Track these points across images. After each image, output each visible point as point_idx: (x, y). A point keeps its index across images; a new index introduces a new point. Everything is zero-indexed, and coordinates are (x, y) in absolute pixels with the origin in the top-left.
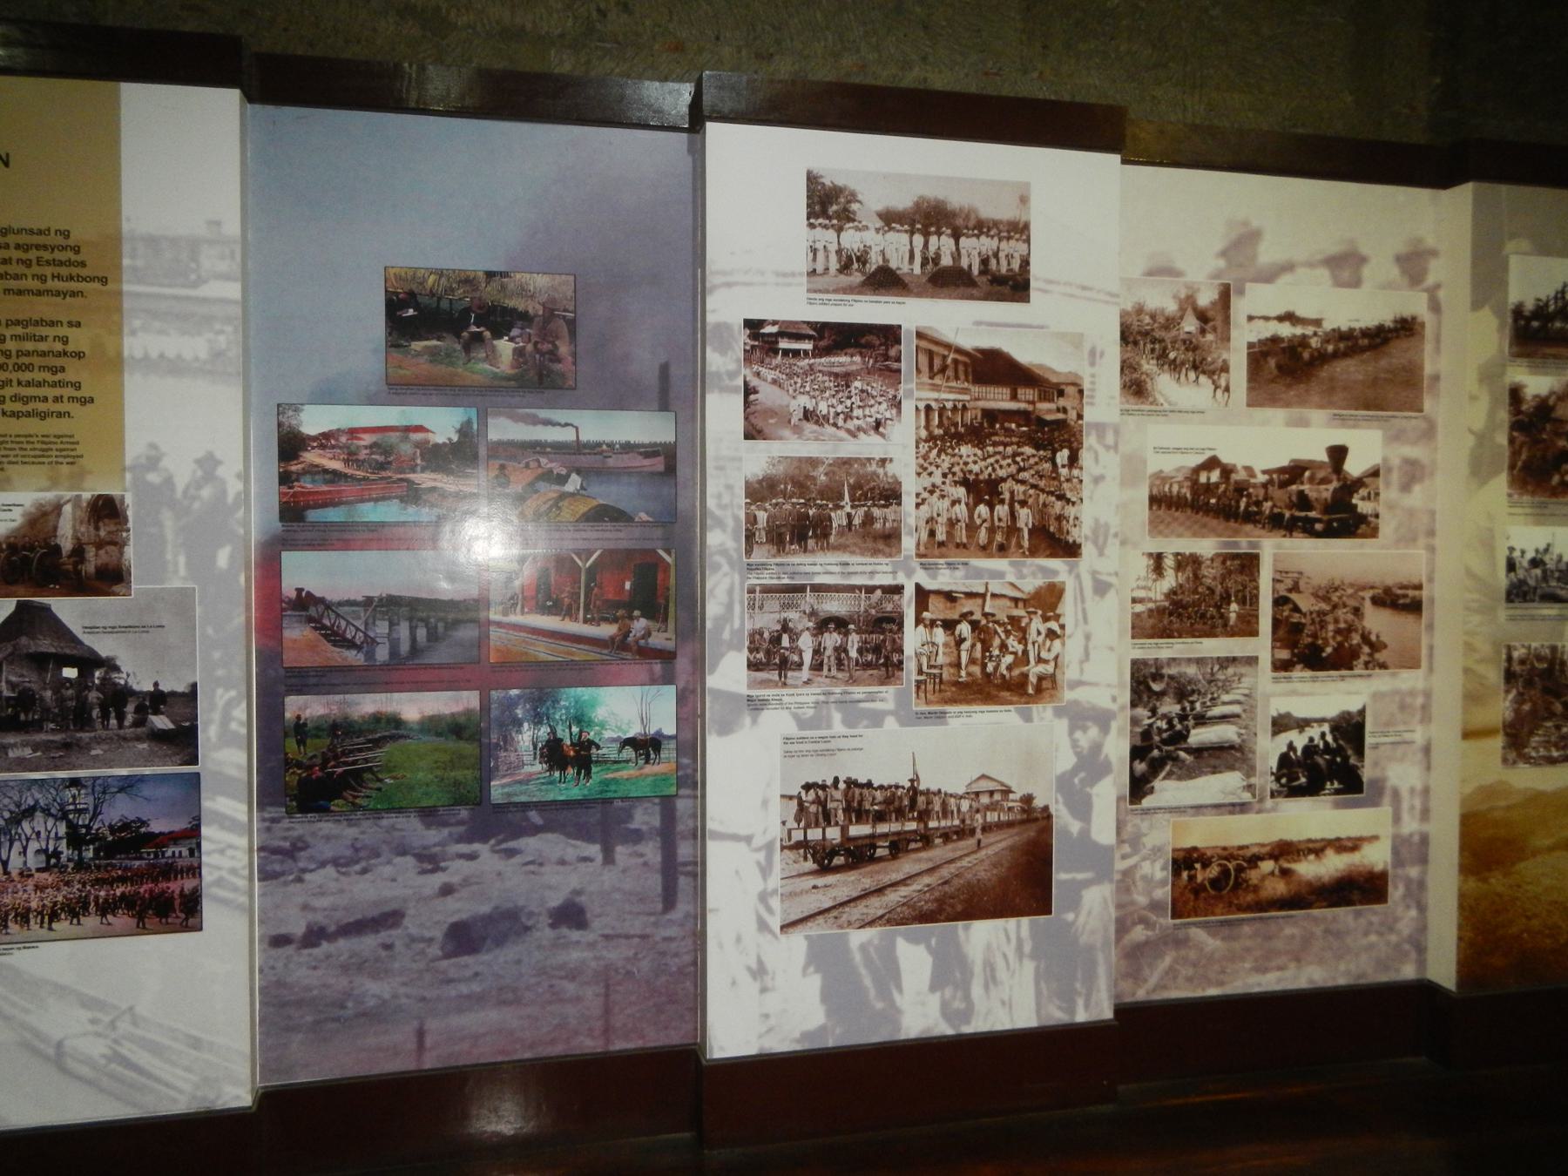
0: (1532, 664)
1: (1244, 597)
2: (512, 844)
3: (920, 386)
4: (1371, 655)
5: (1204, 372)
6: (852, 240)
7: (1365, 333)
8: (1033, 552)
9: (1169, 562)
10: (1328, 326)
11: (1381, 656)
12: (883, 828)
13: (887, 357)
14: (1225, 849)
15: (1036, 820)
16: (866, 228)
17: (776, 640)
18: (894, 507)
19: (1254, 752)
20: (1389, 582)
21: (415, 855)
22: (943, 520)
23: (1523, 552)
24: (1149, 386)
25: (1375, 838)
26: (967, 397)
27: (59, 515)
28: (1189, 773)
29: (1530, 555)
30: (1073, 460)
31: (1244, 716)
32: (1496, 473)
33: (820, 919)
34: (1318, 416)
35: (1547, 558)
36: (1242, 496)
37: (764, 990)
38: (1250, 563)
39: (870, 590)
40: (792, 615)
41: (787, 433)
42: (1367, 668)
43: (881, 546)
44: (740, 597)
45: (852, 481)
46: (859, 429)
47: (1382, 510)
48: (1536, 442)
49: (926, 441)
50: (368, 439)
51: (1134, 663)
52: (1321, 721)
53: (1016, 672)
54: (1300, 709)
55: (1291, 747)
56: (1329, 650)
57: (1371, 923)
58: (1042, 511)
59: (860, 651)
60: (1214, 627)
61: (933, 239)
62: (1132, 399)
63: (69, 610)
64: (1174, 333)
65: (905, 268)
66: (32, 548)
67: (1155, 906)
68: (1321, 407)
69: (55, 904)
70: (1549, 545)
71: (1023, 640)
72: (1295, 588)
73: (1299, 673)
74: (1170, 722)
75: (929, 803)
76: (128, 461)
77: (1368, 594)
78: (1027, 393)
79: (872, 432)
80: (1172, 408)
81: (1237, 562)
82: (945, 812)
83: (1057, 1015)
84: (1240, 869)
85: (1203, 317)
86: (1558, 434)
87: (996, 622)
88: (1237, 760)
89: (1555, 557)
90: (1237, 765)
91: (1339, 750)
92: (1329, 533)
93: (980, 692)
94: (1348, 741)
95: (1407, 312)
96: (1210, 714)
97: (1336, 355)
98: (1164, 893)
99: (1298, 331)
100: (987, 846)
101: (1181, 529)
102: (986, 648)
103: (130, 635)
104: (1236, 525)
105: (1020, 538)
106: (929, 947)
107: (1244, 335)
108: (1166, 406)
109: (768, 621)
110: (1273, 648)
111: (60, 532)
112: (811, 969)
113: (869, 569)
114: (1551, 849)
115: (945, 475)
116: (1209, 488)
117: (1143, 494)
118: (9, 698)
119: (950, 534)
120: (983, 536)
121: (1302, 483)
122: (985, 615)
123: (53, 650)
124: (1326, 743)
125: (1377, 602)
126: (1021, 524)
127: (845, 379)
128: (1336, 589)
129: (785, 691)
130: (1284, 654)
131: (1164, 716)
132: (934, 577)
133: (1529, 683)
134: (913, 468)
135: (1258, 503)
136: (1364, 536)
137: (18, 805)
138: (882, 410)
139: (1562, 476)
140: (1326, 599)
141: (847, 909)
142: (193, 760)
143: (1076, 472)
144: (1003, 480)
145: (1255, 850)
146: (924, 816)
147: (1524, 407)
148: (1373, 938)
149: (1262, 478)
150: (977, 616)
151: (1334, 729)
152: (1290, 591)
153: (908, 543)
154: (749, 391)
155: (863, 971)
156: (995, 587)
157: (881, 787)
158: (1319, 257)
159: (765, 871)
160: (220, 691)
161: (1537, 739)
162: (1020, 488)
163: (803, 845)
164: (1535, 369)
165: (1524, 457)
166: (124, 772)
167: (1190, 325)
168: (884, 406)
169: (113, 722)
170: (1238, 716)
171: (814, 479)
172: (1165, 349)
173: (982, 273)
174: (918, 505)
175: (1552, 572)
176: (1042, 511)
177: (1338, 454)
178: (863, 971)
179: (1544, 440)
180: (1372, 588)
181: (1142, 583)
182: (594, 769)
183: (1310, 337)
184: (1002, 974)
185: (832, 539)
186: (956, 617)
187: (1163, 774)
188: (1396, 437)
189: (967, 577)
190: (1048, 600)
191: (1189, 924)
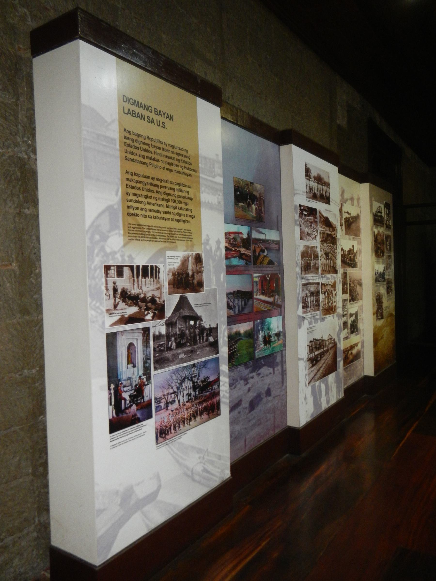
17: (306, 299)
22: (323, 264)
26: (325, 230)
27: (188, 261)
30: (336, 247)
37: (306, 404)
39: (316, 283)
44: (301, 286)
63: (191, 297)
66: (182, 274)
69: (190, 414)
76: (203, 241)
103: (204, 307)
111: (189, 268)
118: (179, 334)
119: (324, 267)
123: (188, 314)
127: (311, 223)
132: (323, 280)
137: (181, 378)
142: (217, 353)
150: (328, 291)
157: (319, 340)
160: (222, 326)
162: (331, 255)
166: (203, 359)
169: (201, 340)
171: (308, 252)
176: (333, 262)
182: (271, 344)
189: (326, 280)
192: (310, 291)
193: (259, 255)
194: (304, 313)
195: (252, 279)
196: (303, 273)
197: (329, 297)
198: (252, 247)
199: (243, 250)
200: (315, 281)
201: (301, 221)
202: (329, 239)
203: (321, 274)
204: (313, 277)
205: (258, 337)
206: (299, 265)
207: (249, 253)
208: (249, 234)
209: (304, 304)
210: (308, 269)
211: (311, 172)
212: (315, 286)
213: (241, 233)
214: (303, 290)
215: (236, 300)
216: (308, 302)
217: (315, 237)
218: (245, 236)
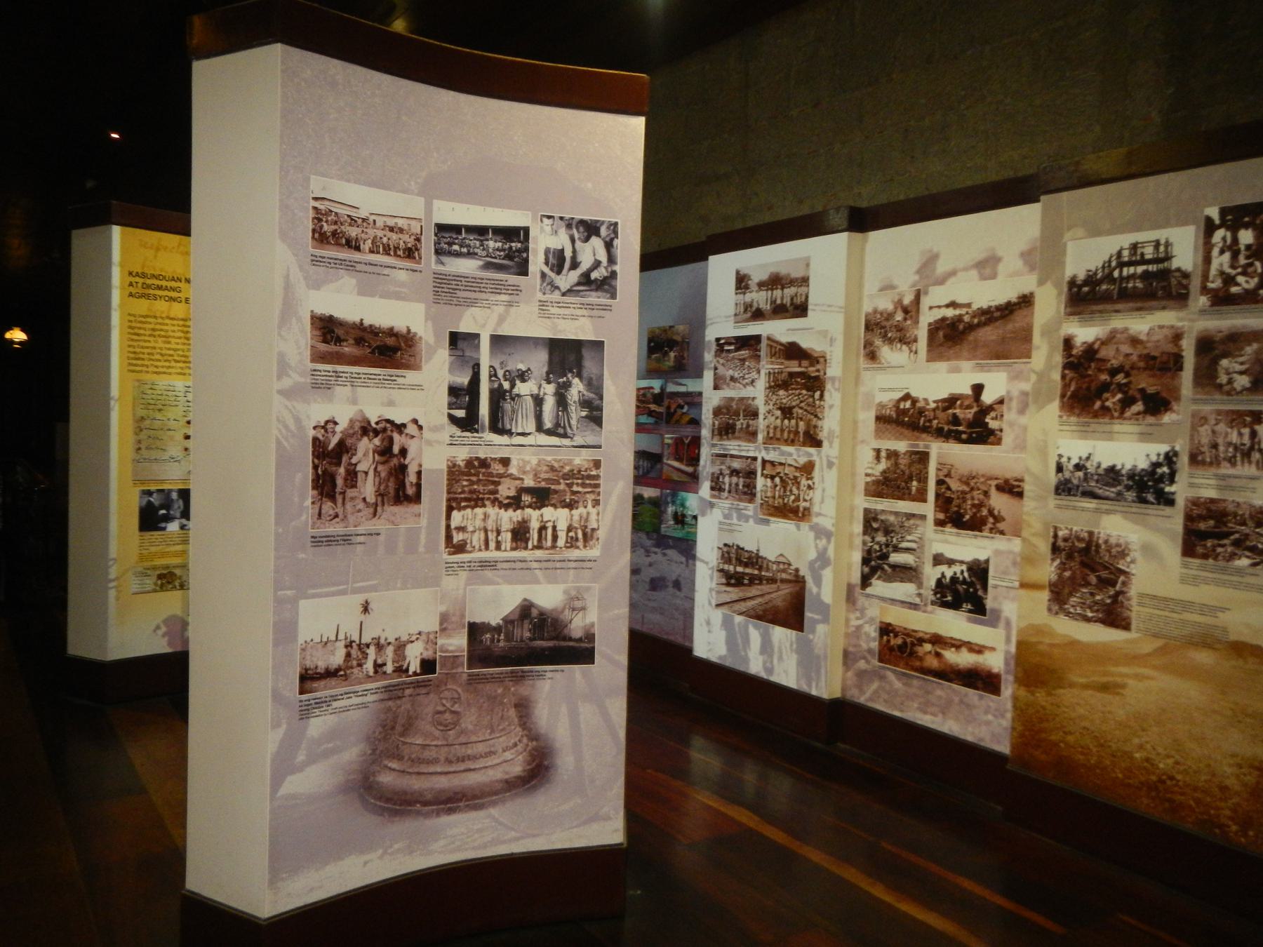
0: (1073, 543)
1: (920, 478)
4: (994, 524)
5: (905, 343)
6: (748, 297)
7: (998, 308)
8: (804, 444)
9: (883, 454)
10: (975, 307)
11: (1001, 526)
12: (748, 571)
14: (905, 629)
15: (799, 581)
17: (718, 478)
19: (922, 573)
20: (1008, 476)
22: (772, 426)
23: (1069, 459)
24: (878, 354)
25: (993, 649)
28: (889, 579)
29: (1075, 461)
30: (822, 396)
31: (918, 550)
32: (1050, 401)
33: (726, 606)
34: (966, 365)
35: (1088, 465)
36: (921, 416)
37: (709, 631)
38: (923, 457)
39: (747, 458)
40: (723, 467)
41: (725, 386)
42: (991, 533)
43: (751, 438)
45: (743, 407)
46: (747, 384)
47: (1005, 427)
48: (1083, 376)
51: (867, 511)
52: (962, 562)
53: (795, 505)
54: (950, 553)
55: (943, 575)
56: (967, 517)
57: (989, 707)
58: (808, 423)
59: (744, 486)
60: (904, 494)
62: (870, 362)
64: (891, 322)
67: (870, 651)
68: (969, 359)
70: (1090, 454)
71: (798, 488)
72: (948, 475)
73: (949, 529)
74: (881, 547)
75: (762, 562)
77: (994, 483)
78: (805, 363)
80: (888, 365)
81: (917, 456)
82: (768, 570)
83: (804, 688)
84: (913, 644)
85: (906, 311)
86: (1100, 370)
88: (913, 576)
89: (1095, 464)
90: (914, 580)
91: (971, 584)
92: (970, 441)
93: (781, 512)
94: (979, 579)
95: (1026, 291)
96: (900, 546)
97: (979, 325)
98: (875, 645)
99: (957, 312)
101: (889, 436)
102: (785, 492)
104: (918, 434)
105: (799, 437)
107: (927, 318)
108: (886, 365)
109: (716, 469)
110: (935, 511)
113: (747, 448)
114: (1086, 687)
115: (774, 405)
116: (905, 412)
117: (872, 415)
119: (774, 433)
120: (786, 435)
121: (955, 409)
122: (786, 474)
124: (964, 578)
125: (999, 488)
126: (800, 430)
127: (743, 360)
128: (974, 478)
130: (941, 516)
131: (878, 543)
132: (768, 454)
133: (1070, 557)
134: (763, 402)
135: (930, 421)
136: (992, 444)
138: (754, 375)
139: (1103, 402)
140: (967, 484)
143: (822, 403)
144: (794, 407)
145: (921, 635)
146: (760, 569)
147: (1074, 352)
148: (990, 717)
149: (933, 405)
150: (782, 475)
151: (969, 569)
152: (946, 476)
153: (760, 437)
154: (716, 369)
156: (790, 461)
158: (972, 263)
159: (712, 578)
161: (1075, 599)
162: (800, 411)
164: (1084, 322)
165: (1072, 388)
167: (899, 317)
170: (914, 550)
171: (732, 407)
172: (886, 332)
173: (792, 304)
175: (1092, 475)
176: (808, 423)
177: (978, 389)
178: (738, 636)
179: (1090, 376)
180: (996, 479)
181: (870, 465)
183: (964, 315)
184: (785, 657)
185: (737, 434)
186: (774, 474)
187: (876, 576)
188: (1016, 377)
190: (808, 468)
191: (887, 668)
192: (729, 467)
193: (675, 411)
194: (713, 496)
195: (663, 441)
196: (717, 438)
197: (785, 488)
198: (666, 402)
199: (653, 407)
200: (744, 454)
202: (796, 381)
203: (764, 443)
204: (739, 446)
205: (666, 509)
206: (708, 426)
208: (663, 389)
210: (727, 434)
211: (752, 277)
213: (652, 388)
214: (713, 462)
215: (641, 460)
216: (723, 483)
217: (753, 381)
218: (657, 390)
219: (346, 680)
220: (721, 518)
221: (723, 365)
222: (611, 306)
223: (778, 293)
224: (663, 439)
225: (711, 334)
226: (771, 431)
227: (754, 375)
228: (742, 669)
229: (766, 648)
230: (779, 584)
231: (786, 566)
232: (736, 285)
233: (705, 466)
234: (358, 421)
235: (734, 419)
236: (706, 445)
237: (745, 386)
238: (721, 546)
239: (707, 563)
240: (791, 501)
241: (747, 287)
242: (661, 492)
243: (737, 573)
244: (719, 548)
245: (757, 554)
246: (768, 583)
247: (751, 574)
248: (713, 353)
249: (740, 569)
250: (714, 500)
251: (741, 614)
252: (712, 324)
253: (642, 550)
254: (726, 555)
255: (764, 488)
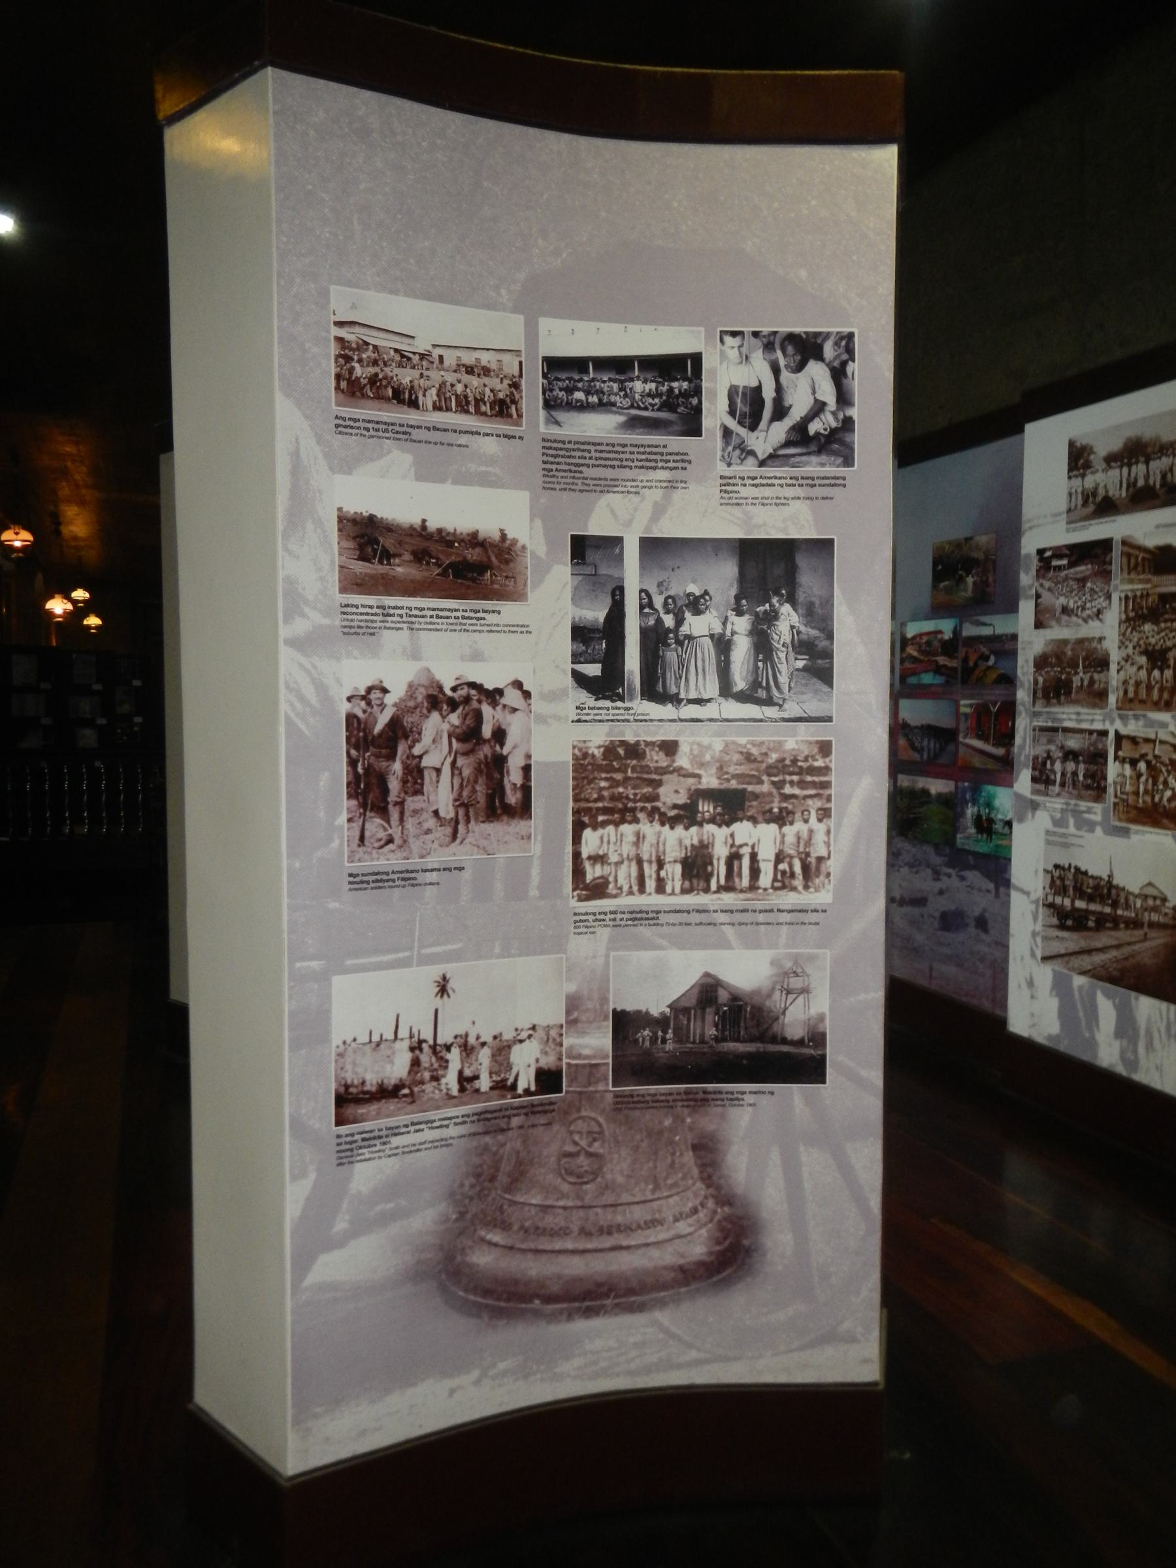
2: (962, 873)
3: (1123, 581)
6: (1090, 481)
12: (1093, 907)
13: (1105, 563)
16: (1097, 471)
17: (1044, 764)
18: (1105, 672)
21: (933, 869)
22: (1132, 682)
33: (1059, 960)
37: (1032, 997)
39: (1091, 732)
40: (1052, 747)
41: (1053, 623)
43: (1097, 701)
44: (1030, 733)
45: (1084, 654)
46: (1089, 616)
49: (1125, 622)
50: (925, 639)
59: (1084, 776)
61: (1134, 468)
65: (1117, 494)
75: (1118, 895)
79: (1095, 618)
82: (1127, 906)
87: (1162, 763)
100: (1151, 939)
102: (1155, 783)
106: (1114, 1002)
109: (1040, 750)
112: (1054, 993)
113: (1090, 717)
115: (1134, 648)
119: (1136, 693)
120: (1155, 694)
122: (1156, 757)
127: (1082, 581)
129: (1047, 799)
132: (1125, 725)
138: (1101, 602)
141: (1072, 958)
146: (1115, 905)
150: (1150, 757)
153: (1112, 699)
154: (1038, 596)
155: (1079, 1006)
156: (1163, 735)
157: (1092, 877)
159: (1035, 918)
163: (1051, 906)
168: (1102, 599)
171: (1064, 654)
173: (1162, 486)
174: (1118, 671)
178: (1079, 1006)
182: (994, 837)
184: (1156, 1043)
186: (1137, 756)
189: (1145, 726)
193: (976, 665)
194: (1035, 792)
198: (962, 652)
199: (942, 660)
200: (1085, 726)
201: (1041, 585)
207: (954, 664)
208: (956, 632)
209: (1037, 773)
210: (1057, 695)
212: (1084, 738)
213: (940, 632)
214: (1035, 740)
215: (926, 740)
217: (1099, 612)
218: (948, 635)
219: (413, 1102)
220: (1048, 824)
221: (1050, 589)
222: (844, 479)
223: (1139, 469)
224: (957, 706)
225: (1030, 544)
226: (1131, 689)
227: (1101, 602)
228: (1085, 1057)
229: (1126, 1027)
230: (1146, 929)
231: (1158, 902)
232: (1069, 464)
233: (1022, 747)
234: (423, 686)
235: (1069, 673)
236: (1024, 714)
237: (1085, 621)
238: (1050, 868)
239: (1028, 894)
240: (1165, 799)
241: (1088, 466)
242: (956, 787)
243: (1074, 909)
244: (1046, 871)
245: (1109, 882)
246: (1127, 927)
247: (1101, 913)
248: (1034, 573)
249: (1080, 904)
250: (1039, 798)
251: (1083, 973)
252: (1031, 528)
253: (929, 871)
254: (1058, 882)
255: (1119, 779)
